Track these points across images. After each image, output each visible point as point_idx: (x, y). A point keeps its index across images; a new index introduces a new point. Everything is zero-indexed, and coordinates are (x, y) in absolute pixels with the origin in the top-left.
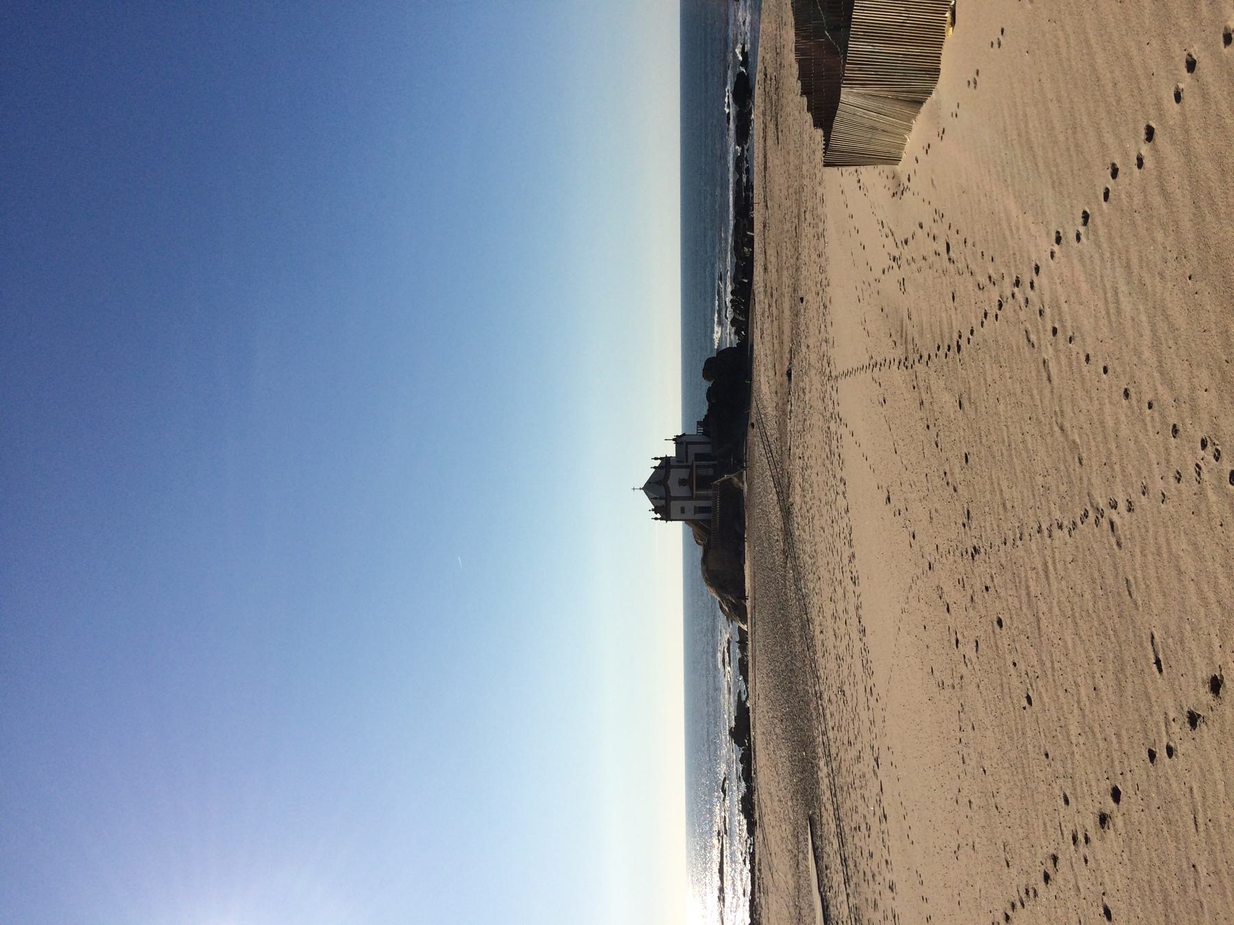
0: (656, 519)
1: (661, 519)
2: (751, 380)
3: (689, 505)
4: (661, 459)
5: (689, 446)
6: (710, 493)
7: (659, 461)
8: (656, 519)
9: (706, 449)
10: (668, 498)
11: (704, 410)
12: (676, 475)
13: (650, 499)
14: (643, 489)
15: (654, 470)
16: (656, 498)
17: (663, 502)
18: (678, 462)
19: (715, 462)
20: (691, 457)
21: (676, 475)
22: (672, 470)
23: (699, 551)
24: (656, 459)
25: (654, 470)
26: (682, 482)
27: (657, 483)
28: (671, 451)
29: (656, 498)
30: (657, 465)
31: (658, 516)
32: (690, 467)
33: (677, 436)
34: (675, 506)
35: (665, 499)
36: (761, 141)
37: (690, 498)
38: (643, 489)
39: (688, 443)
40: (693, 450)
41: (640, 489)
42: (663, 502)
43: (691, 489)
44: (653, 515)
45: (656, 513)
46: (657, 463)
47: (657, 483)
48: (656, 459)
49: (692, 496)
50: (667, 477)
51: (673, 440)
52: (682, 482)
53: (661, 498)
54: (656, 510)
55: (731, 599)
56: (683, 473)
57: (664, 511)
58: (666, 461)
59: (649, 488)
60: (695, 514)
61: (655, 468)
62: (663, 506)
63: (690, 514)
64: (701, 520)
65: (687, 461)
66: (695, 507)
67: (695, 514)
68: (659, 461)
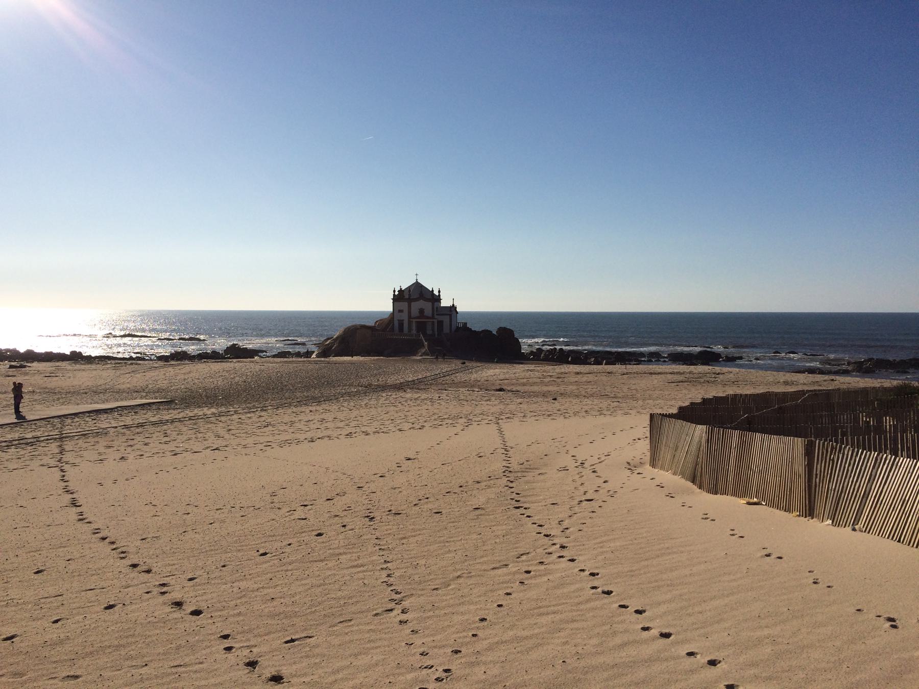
0: (394, 291)
1: (394, 295)
2: (497, 362)
3: (405, 317)
4: (439, 295)
6: (414, 332)
7: (437, 294)
8: (394, 291)
9: (446, 330)
10: (410, 300)
11: (476, 327)
12: (427, 307)
13: (409, 287)
14: (417, 281)
15: (431, 290)
16: (410, 291)
17: (407, 297)
18: (437, 308)
19: (436, 336)
20: (441, 318)
21: (427, 307)
22: (430, 303)
23: (372, 324)
24: (439, 292)
25: (431, 290)
26: (421, 311)
27: (421, 292)
28: (445, 302)
29: (410, 291)
30: (434, 292)
31: (397, 293)
32: (433, 317)
33: (456, 307)
34: (404, 305)
35: (409, 298)
36: (671, 371)
37: (410, 317)
38: (417, 281)
39: (450, 315)
40: (446, 320)
41: (417, 280)
42: (407, 297)
43: (415, 318)
44: (397, 289)
46: (436, 293)
47: (421, 292)
48: (439, 292)
49: (411, 318)
50: (427, 300)
51: (453, 305)
52: (421, 311)
53: (410, 295)
54: (401, 291)
55: (335, 346)
56: (428, 312)
57: (400, 297)
58: (438, 299)
59: (417, 286)
61: (433, 291)
62: (404, 297)
63: (398, 317)
64: (393, 325)
65: (437, 315)
66: (403, 320)
67: (398, 320)
68: (437, 294)
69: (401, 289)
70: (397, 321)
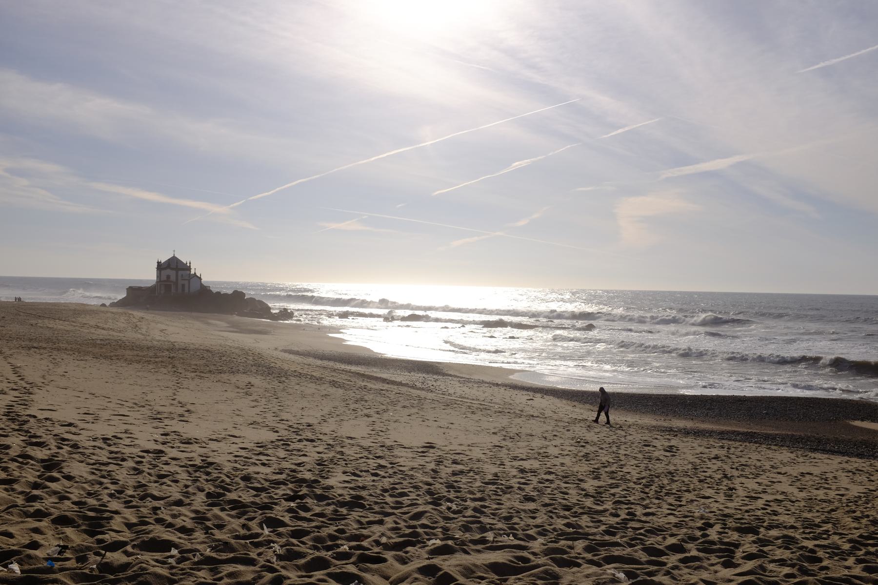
4: (190, 266)
9: (186, 290)
11: (214, 290)
12: (173, 274)
18: (182, 275)
23: (149, 285)
24: (190, 263)
26: (168, 277)
40: (186, 283)
43: (164, 281)
46: (188, 265)
48: (190, 263)
50: (172, 269)
51: (195, 273)
52: (168, 277)
56: (173, 278)
58: (189, 269)
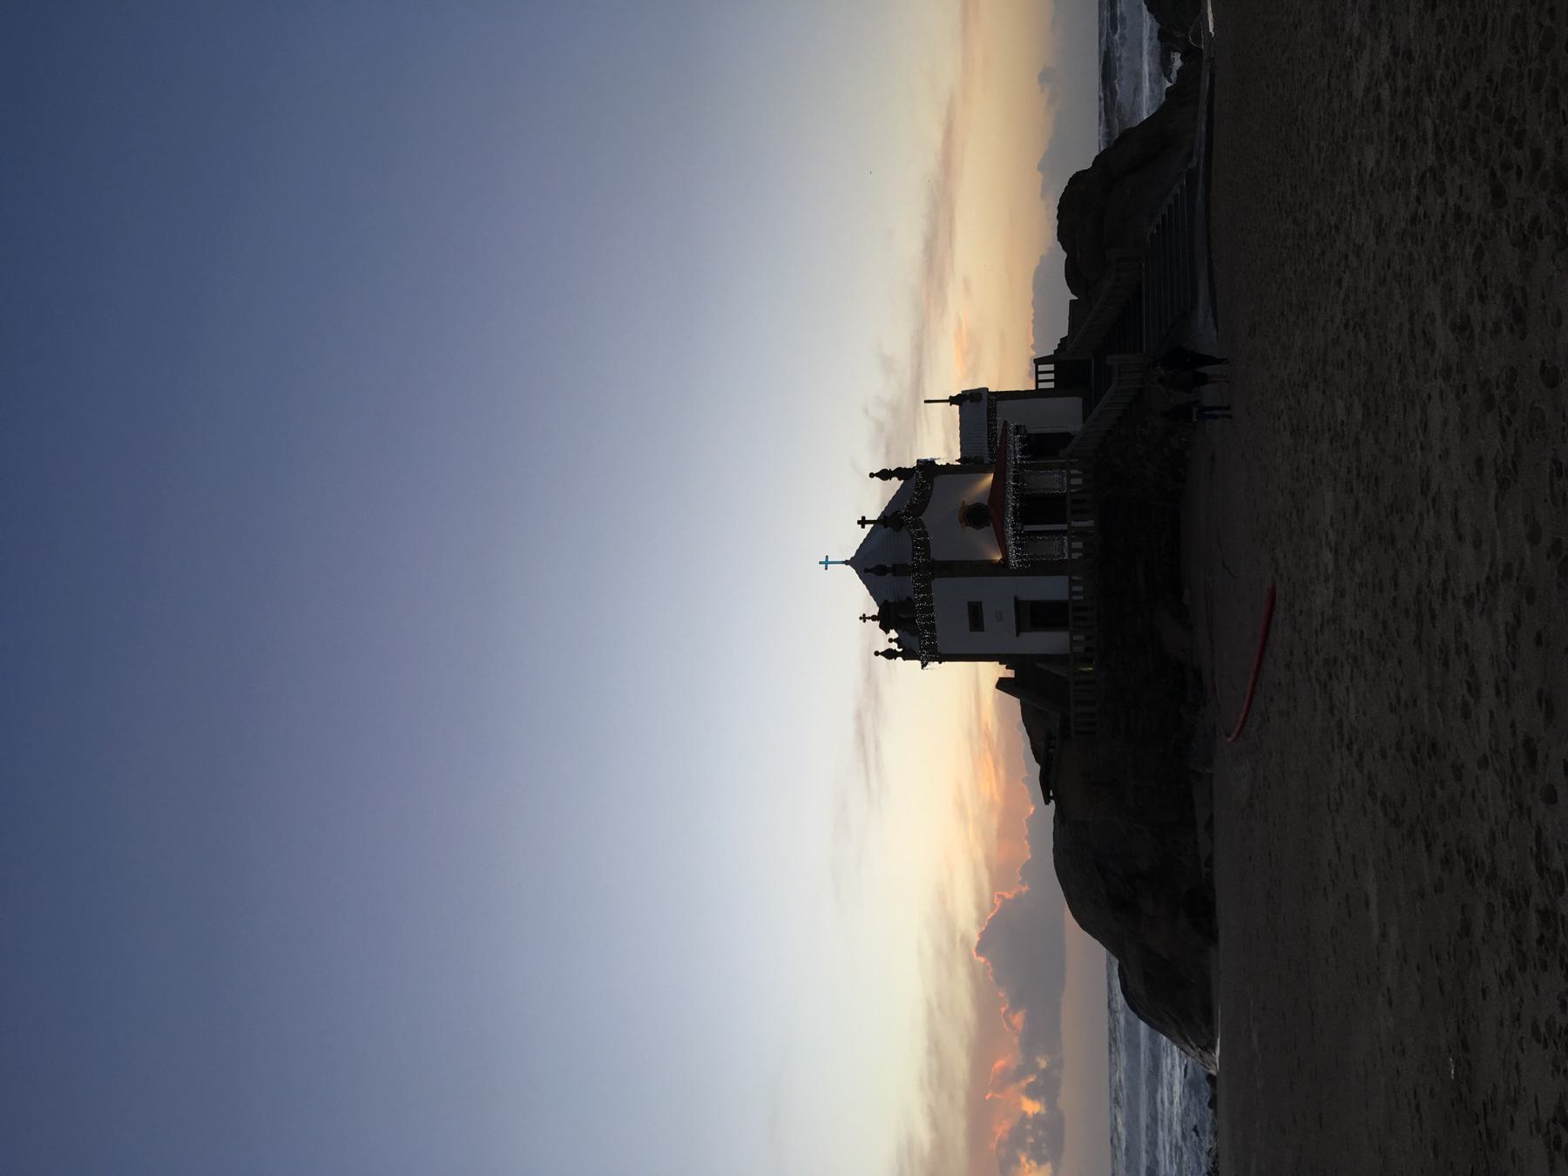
1: (907, 655)
3: (999, 596)
5: (1001, 405)
8: (890, 654)
16: (881, 570)
17: (906, 587)
22: (939, 481)
26: (976, 516)
29: (881, 570)
34: (949, 597)
41: (846, 563)
42: (906, 587)
45: (885, 628)
53: (898, 570)
54: (886, 619)
59: (867, 564)
60: (1017, 635)
66: (1018, 604)
67: (1019, 631)
69: (874, 618)
70: (1022, 633)
